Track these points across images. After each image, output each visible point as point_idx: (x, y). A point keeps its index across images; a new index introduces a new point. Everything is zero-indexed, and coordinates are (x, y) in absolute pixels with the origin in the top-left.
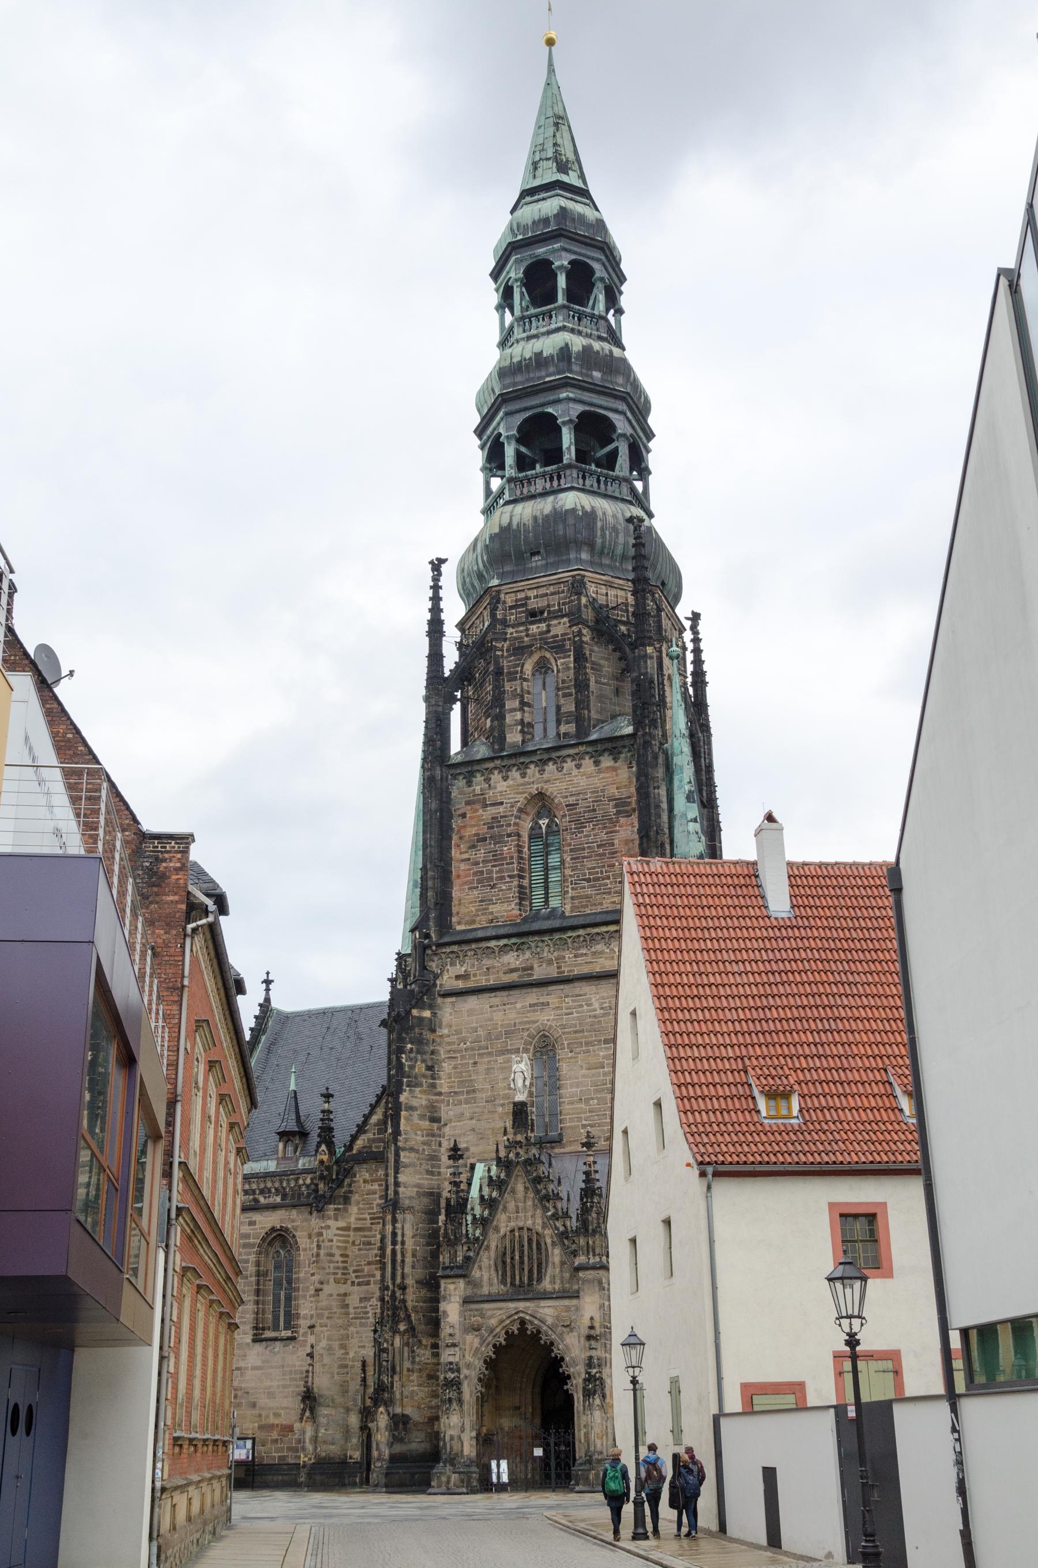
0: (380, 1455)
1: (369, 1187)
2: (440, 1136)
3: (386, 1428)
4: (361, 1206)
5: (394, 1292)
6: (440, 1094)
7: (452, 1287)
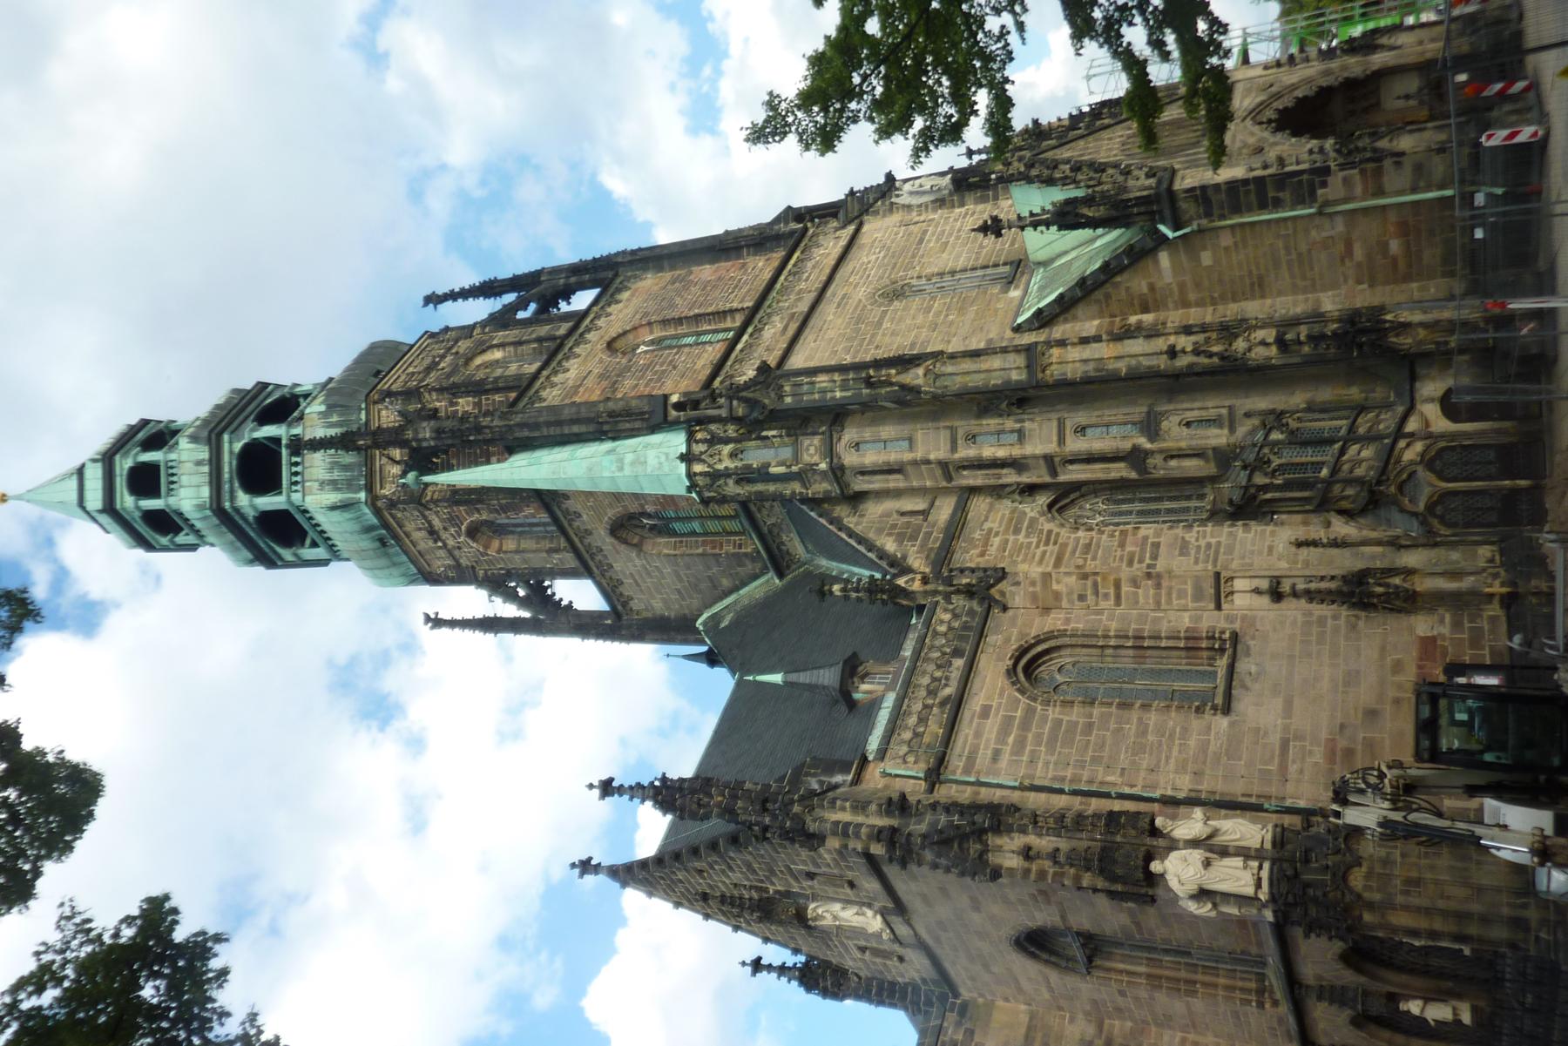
4: (1020, 559)
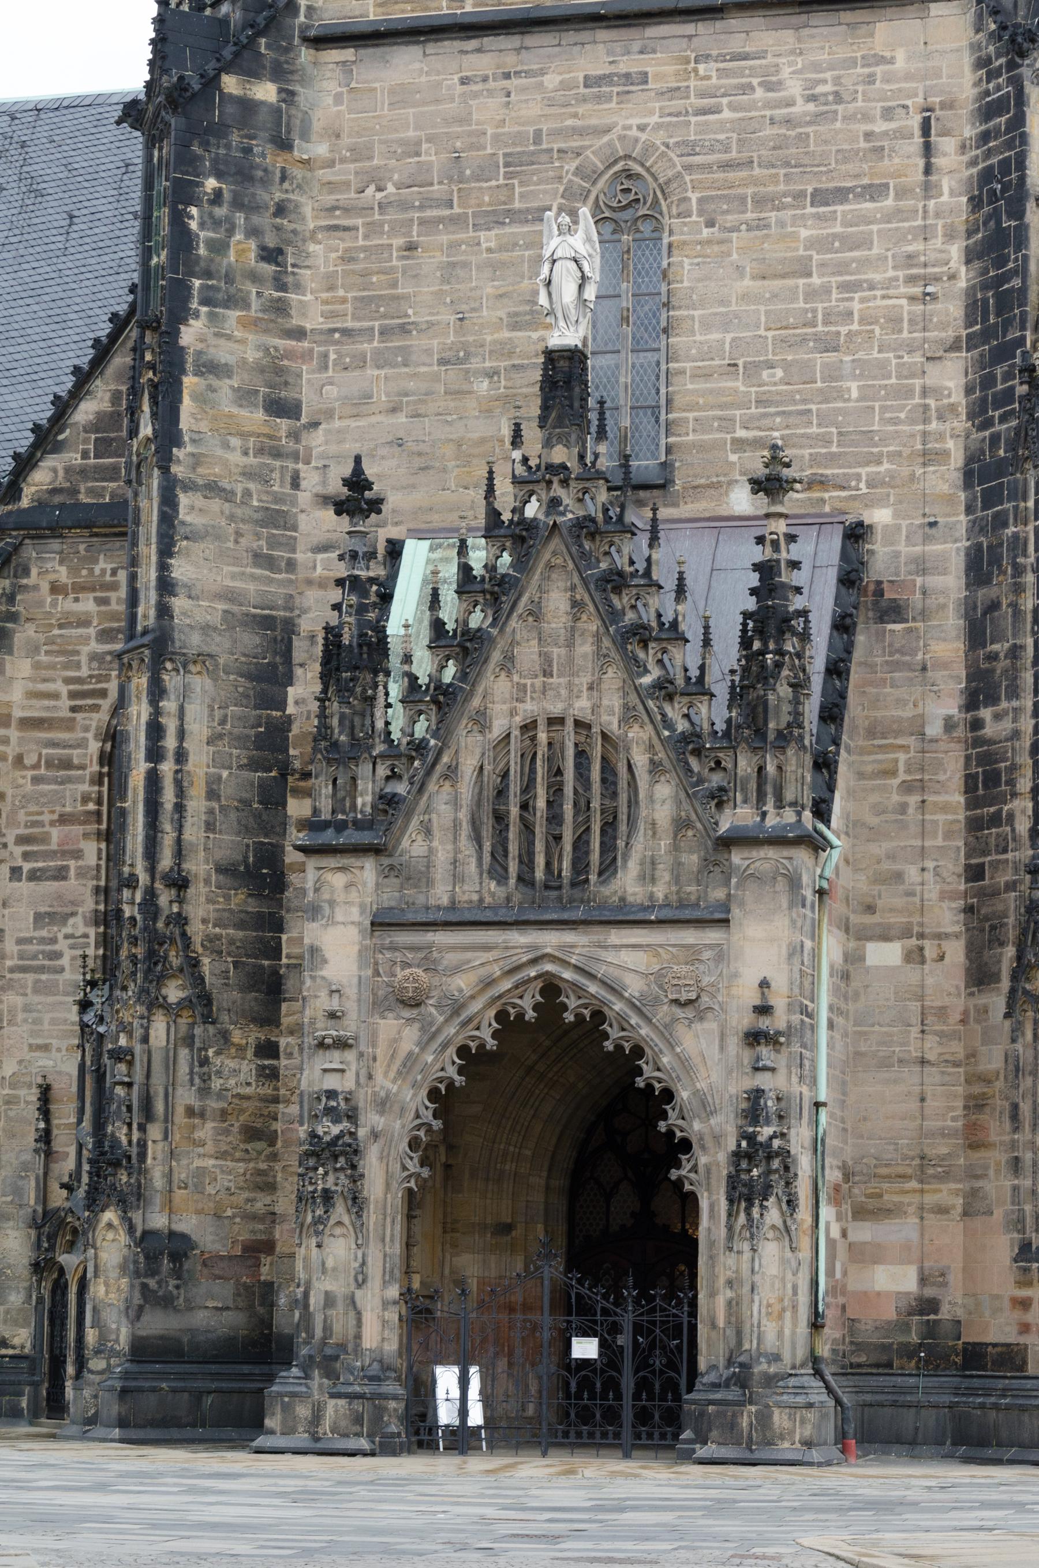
0: (102, 1338)
1: (66, 604)
2: (296, 456)
3: (123, 1268)
4: (43, 658)
5: (151, 894)
6: (299, 334)
7: (338, 880)
